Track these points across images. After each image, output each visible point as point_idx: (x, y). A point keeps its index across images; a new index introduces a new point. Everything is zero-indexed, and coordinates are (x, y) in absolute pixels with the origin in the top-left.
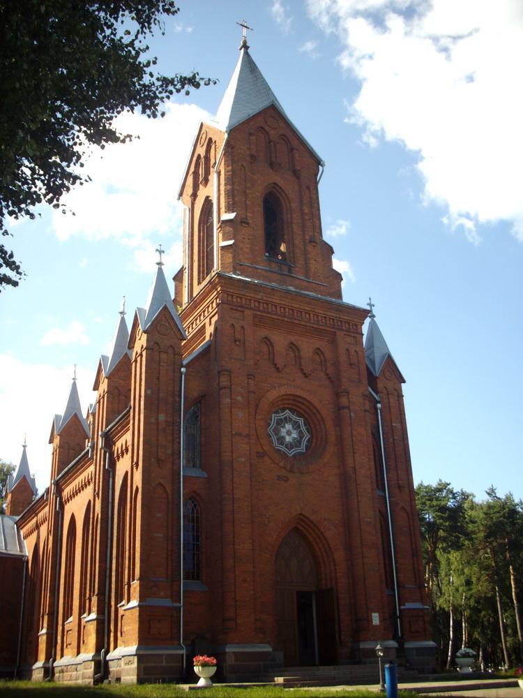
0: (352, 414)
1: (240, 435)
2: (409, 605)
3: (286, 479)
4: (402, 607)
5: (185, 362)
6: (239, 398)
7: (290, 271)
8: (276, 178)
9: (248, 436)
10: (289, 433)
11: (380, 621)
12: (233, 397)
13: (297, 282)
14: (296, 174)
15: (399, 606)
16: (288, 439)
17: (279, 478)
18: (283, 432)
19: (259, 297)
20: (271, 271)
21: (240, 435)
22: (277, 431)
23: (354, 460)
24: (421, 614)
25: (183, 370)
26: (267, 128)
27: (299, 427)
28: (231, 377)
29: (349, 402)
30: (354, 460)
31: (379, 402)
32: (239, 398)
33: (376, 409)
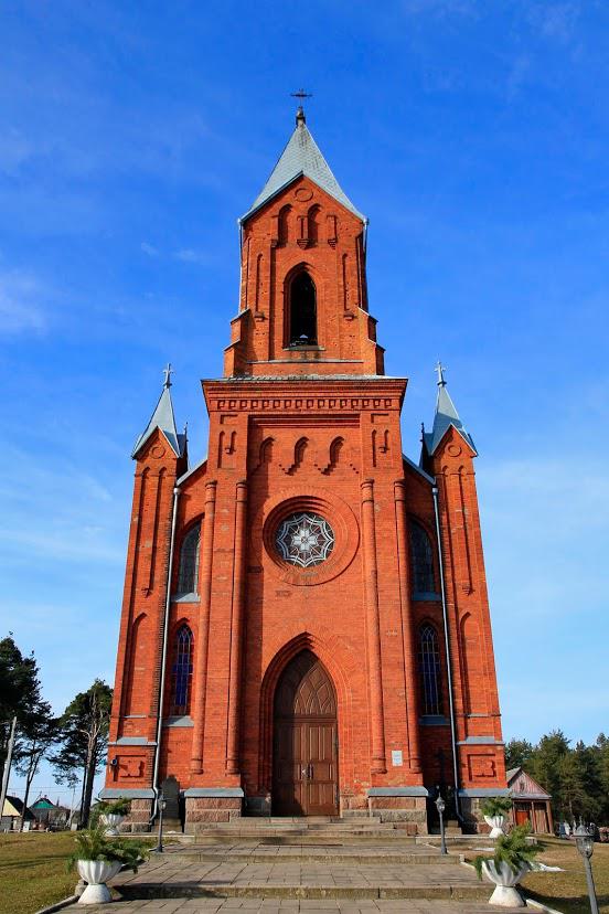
0: (377, 507)
1: (223, 551)
2: (471, 740)
3: (288, 594)
4: (460, 743)
6: (225, 511)
7: (317, 356)
10: (305, 540)
11: (404, 761)
13: (323, 366)
14: (333, 243)
15: (456, 740)
16: (303, 547)
17: (278, 593)
19: (256, 395)
21: (223, 551)
24: (490, 751)
25: (176, 490)
28: (215, 488)
31: (435, 487)
32: (225, 511)
33: (432, 494)
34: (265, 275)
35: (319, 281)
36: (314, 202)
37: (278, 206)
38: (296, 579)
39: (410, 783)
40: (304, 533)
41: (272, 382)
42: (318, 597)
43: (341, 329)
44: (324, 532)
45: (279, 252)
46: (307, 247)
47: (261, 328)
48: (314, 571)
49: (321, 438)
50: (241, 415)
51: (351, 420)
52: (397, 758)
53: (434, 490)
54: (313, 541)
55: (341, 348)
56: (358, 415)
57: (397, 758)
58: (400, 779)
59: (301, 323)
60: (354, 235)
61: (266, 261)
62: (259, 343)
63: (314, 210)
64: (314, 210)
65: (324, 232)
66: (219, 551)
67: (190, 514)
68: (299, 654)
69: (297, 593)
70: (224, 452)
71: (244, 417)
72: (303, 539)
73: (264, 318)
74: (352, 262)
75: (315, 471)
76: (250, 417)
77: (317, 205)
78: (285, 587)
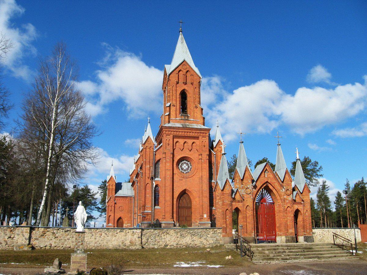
0: (203, 161)
5: (155, 151)
6: (168, 160)
7: (188, 118)
8: (185, 87)
9: (170, 170)
12: (166, 160)
13: (189, 121)
14: (192, 84)
17: (180, 180)
18: (183, 167)
20: (181, 120)
22: (181, 167)
23: (202, 174)
25: (154, 153)
26: (182, 70)
27: (188, 165)
29: (202, 157)
30: (202, 174)
31: (215, 155)
32: (168, 160)
34: (174, 92)
35: (189, 96)
36: (187, 70)
37: (178, 70)
38: (184, 176)
39: (207, 221)
40: (185, 165)
41: (179, 127)
42: (189, 181)
43: (194, 111)
44: (189, 165)
45: (178, 85)
46: (185, 85)
47: (173, 109)
48: (187, 175)
49: (190, 141)
50: (171, 135)
51: (197, 138)
52: (205, 216)
53: (215, 156)
54: (187, 167)
55: (194, 116)
56: (199, 137)
57: (205, 216)
58: (205, 220)
59: (184, 108)
60: (198, 82)
61: (174, 88)
62: (173, 113)
63: (187, 71)
64: (187, 71)
65: (189, 81)
66: (167, 170)
67: (157, 159)
68: (184, 193)
69: (184, 180)
70: (167, 145)
71: (172, 136)
72: (185, 166)
73: (175, 106)
74: (197, 90)
75: (188, 150)
76: (173, 136)
77: (188, 71)
78: (181, 178)
